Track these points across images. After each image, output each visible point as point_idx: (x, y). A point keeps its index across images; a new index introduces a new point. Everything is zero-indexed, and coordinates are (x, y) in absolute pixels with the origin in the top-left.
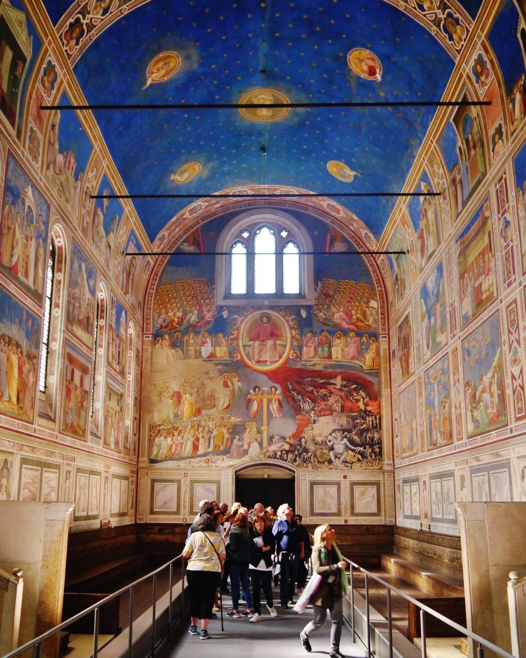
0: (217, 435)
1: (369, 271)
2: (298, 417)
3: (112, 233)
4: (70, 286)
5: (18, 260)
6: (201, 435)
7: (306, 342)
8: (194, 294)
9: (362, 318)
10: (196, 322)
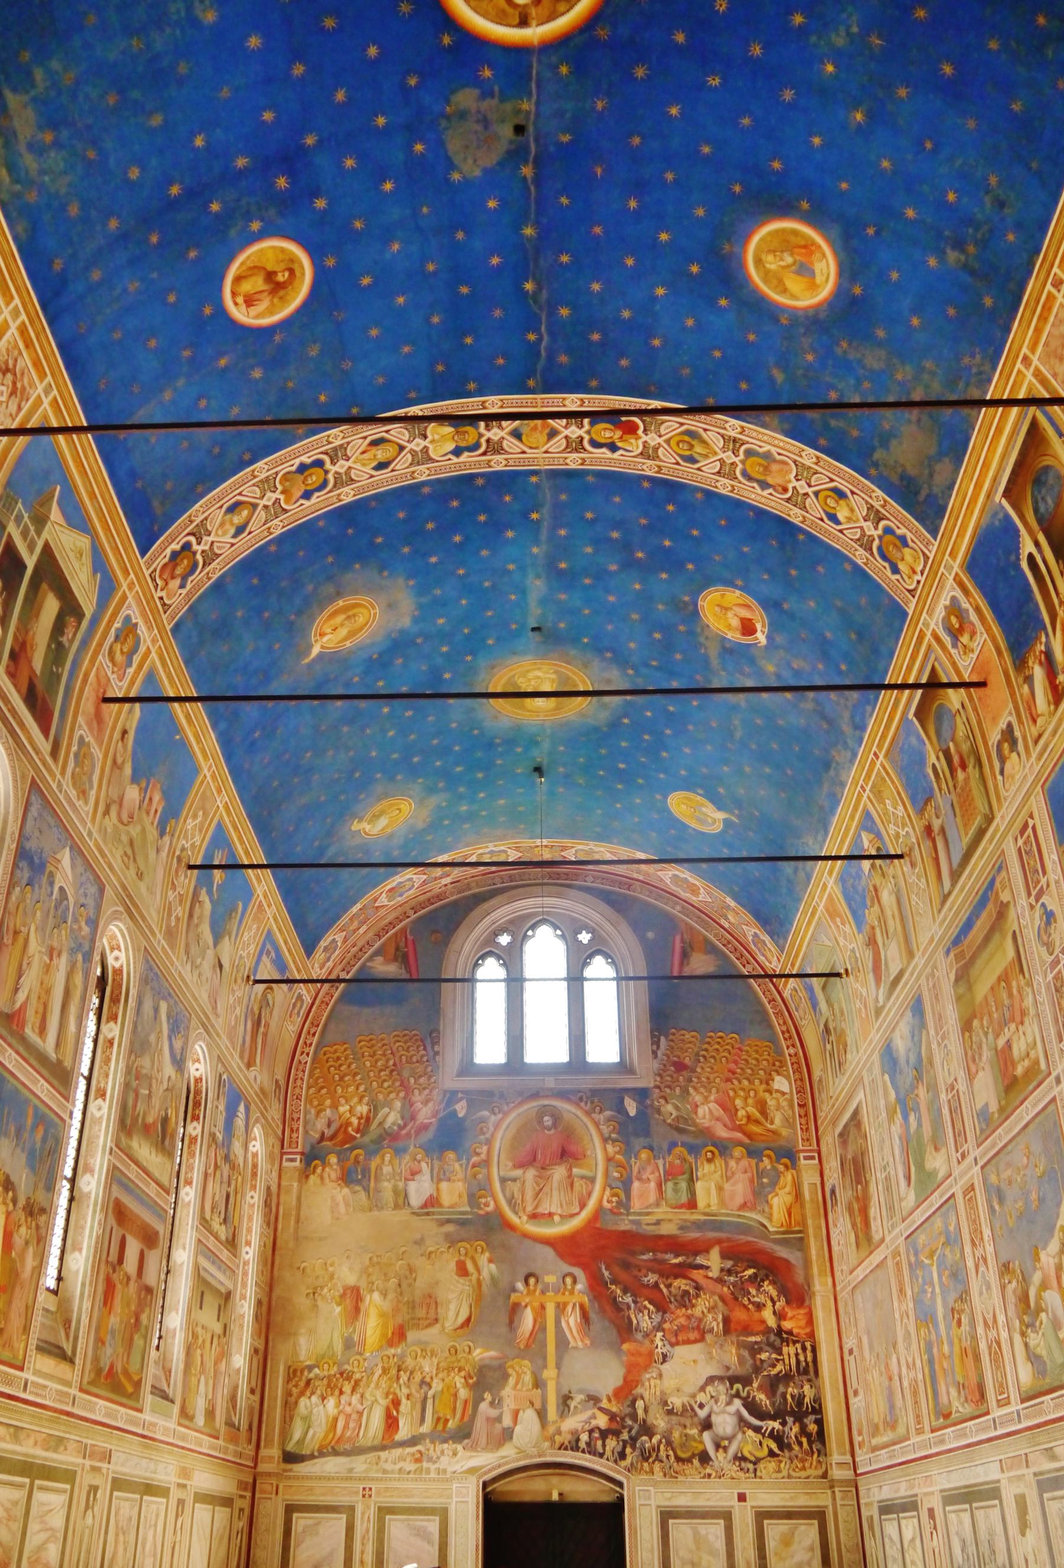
1: (765, 1012)
2: (625, 1347)
3: (227, 938)
4: (131, 1052)
5: (28, 998)
6: (405, 1391)
7: (639, 1172)
9: (758, 1115)
10: (401, 1128)
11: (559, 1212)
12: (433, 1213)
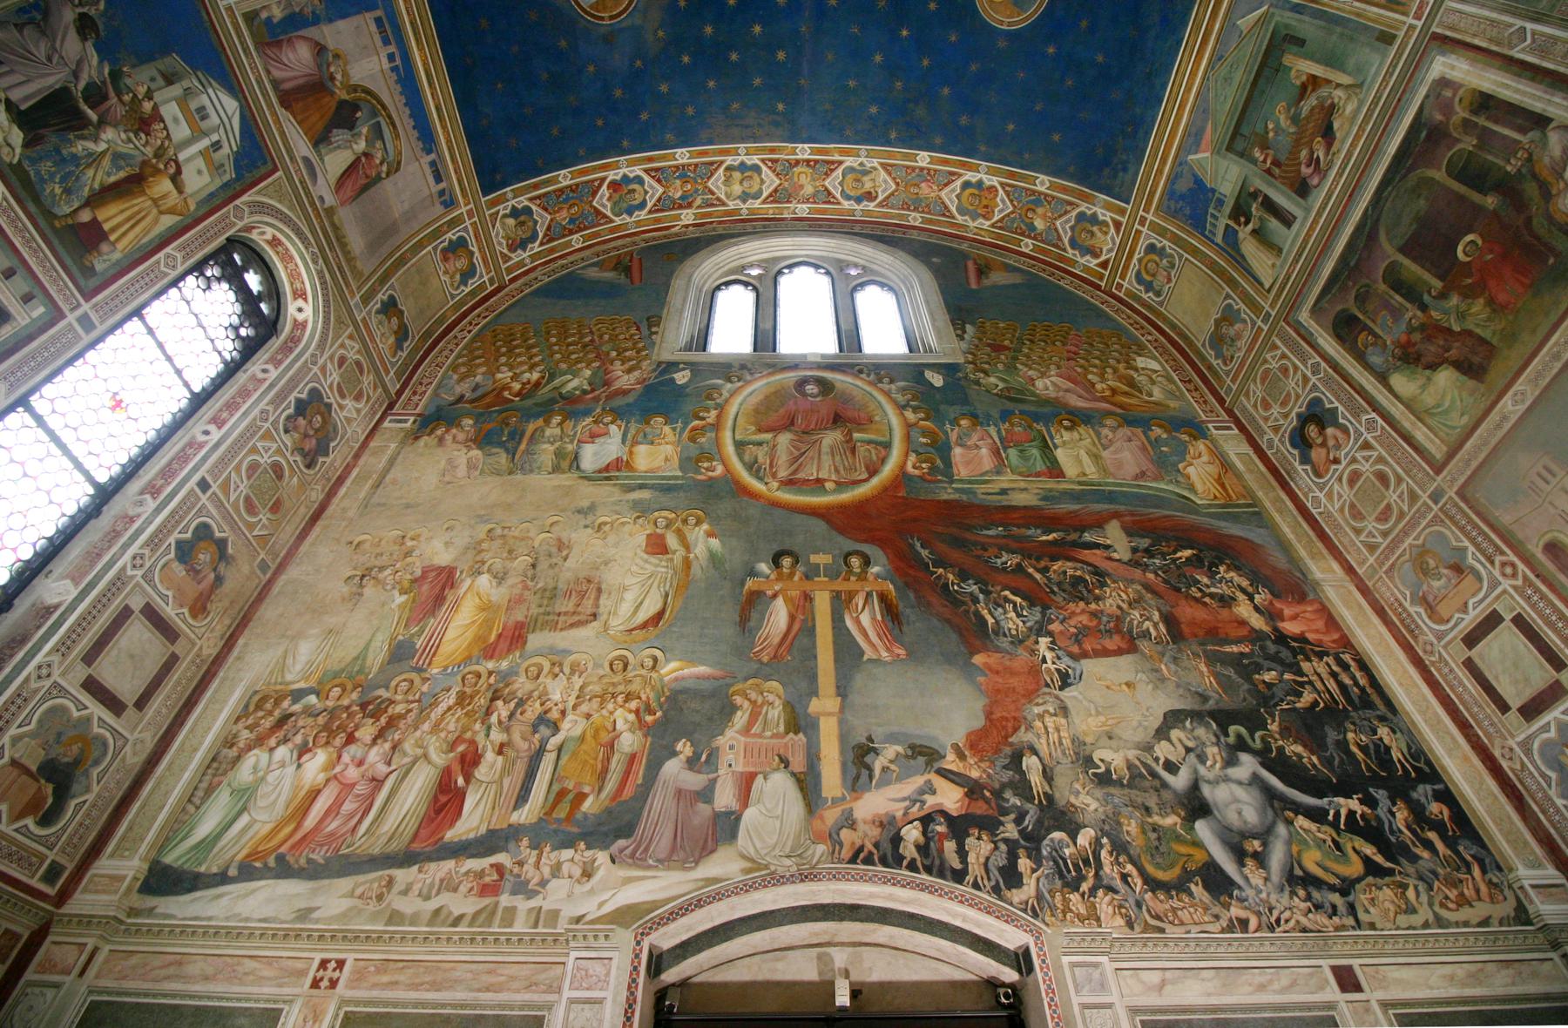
0: (582, 738)
2: (978, 659)
6: (497, 736)
8: (592, 341)
9: (1126, 388)
10: (585, 392)
11: (834, 477)
12: (617, 478)
